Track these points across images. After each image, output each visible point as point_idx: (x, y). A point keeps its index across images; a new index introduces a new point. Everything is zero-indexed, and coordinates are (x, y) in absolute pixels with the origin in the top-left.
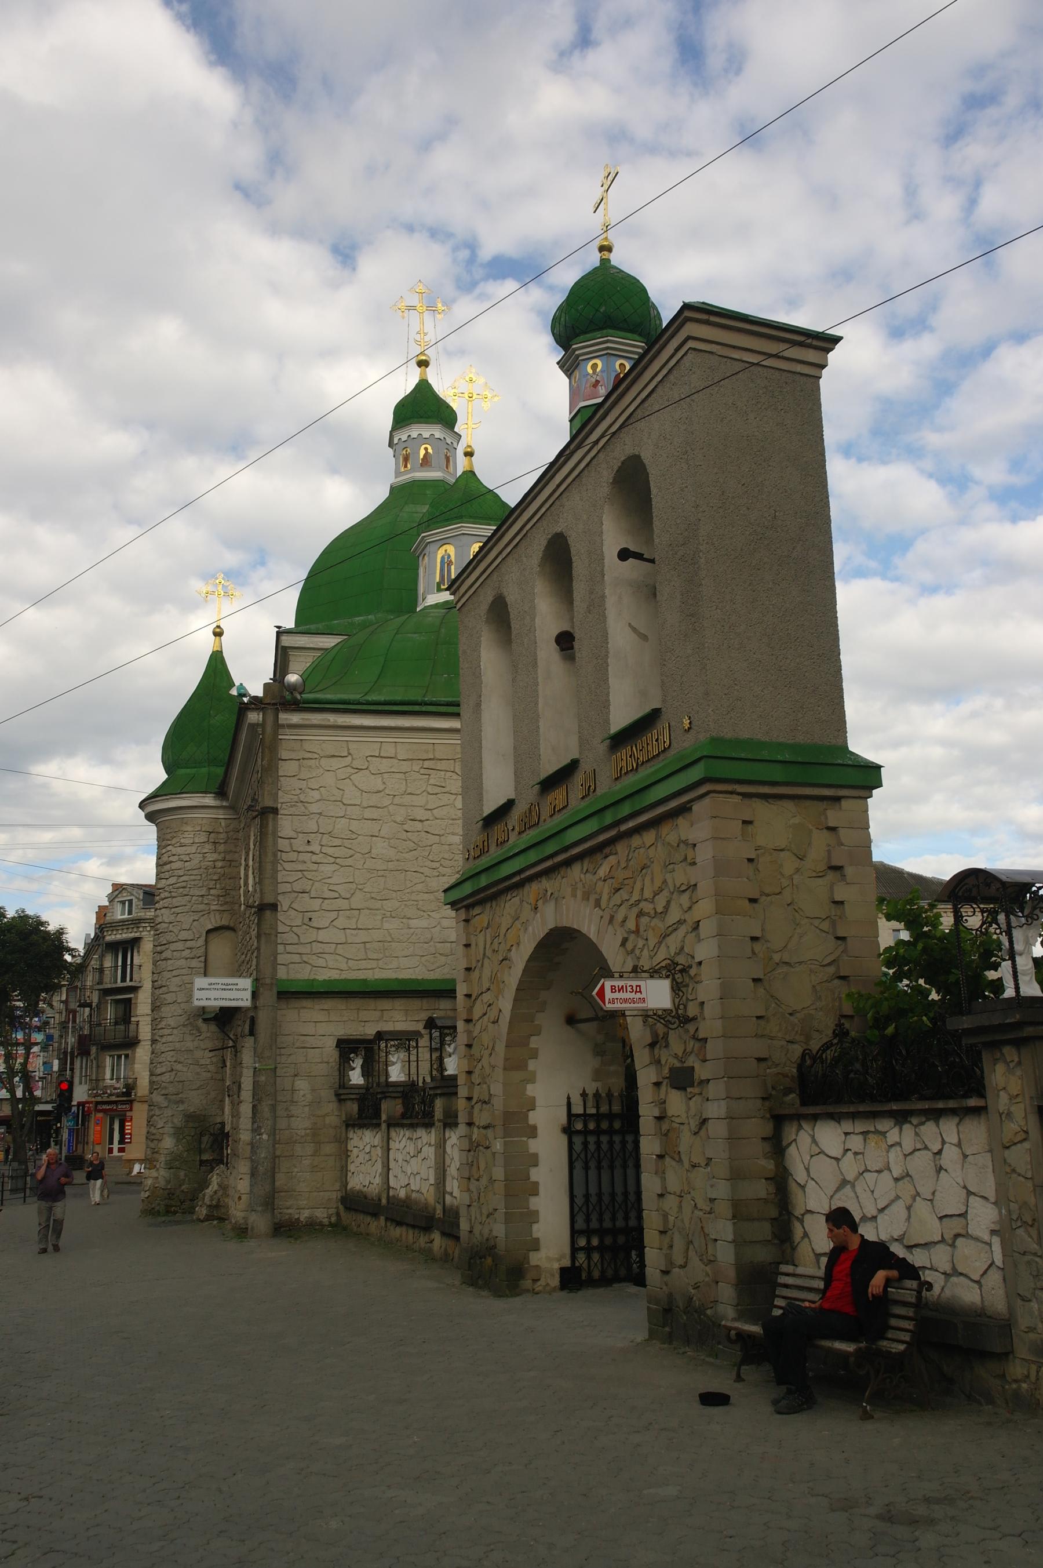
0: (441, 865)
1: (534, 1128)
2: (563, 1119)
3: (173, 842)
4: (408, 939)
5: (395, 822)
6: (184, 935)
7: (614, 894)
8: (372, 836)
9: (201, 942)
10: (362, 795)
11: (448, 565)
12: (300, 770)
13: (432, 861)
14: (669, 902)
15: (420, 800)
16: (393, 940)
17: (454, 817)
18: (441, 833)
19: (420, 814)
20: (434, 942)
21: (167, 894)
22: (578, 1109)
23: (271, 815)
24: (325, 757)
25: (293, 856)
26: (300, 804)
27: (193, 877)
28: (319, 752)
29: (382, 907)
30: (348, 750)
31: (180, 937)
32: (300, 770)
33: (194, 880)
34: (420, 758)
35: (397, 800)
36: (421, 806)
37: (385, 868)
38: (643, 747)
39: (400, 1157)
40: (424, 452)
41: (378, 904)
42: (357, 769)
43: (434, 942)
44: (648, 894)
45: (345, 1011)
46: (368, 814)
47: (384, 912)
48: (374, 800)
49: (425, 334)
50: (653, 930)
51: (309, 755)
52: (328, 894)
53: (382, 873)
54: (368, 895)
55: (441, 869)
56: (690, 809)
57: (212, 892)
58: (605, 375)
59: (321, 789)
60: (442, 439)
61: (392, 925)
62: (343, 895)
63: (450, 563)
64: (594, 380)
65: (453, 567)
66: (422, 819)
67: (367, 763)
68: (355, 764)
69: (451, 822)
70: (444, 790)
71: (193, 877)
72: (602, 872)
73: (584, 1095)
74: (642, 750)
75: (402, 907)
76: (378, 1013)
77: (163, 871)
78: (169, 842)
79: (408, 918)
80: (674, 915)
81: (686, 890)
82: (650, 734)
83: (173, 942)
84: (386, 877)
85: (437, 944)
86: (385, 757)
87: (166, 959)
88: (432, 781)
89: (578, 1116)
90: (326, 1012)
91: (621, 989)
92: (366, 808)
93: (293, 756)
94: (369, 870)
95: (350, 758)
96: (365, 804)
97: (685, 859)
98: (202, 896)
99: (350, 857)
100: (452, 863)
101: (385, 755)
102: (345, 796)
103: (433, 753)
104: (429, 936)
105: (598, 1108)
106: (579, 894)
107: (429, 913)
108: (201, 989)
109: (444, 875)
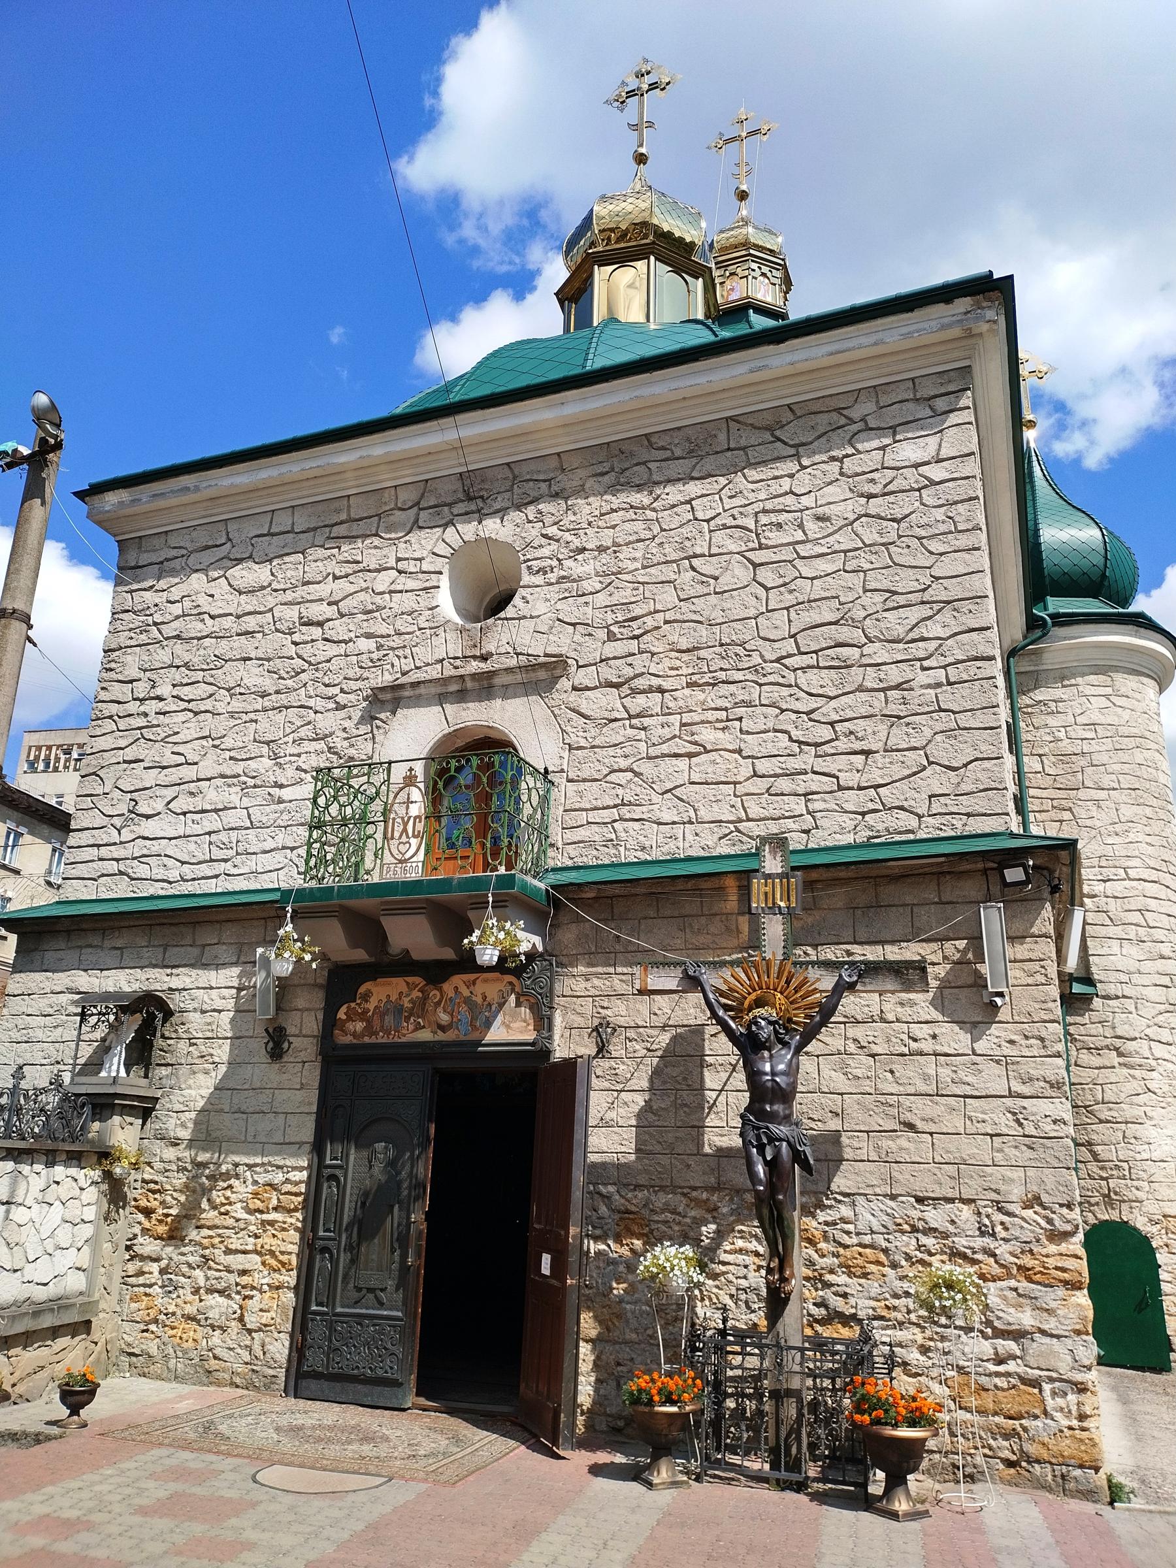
0: (342, 691)
13: (326, 686)
15: (323, 590)
17: (370, 607)
19: (318, 611)
24: (196, 551)
25: (133, 707)
28: (188, 545)
41: (238, 768)
42: (236, 559)
45: (145, 949)
51: (174, 553)
53: (252, 716)
54: (227, 754)
55: (342, 698)
62: (191, 758)
67: (250, 548)
69: (365, 617)
76: (195, 951)
79: (281, 786)
90: (119, 952)
93: (154, 558)
94: (232, 715)
95: (229, 545)
100: (359, 684)
103: (349, 511)
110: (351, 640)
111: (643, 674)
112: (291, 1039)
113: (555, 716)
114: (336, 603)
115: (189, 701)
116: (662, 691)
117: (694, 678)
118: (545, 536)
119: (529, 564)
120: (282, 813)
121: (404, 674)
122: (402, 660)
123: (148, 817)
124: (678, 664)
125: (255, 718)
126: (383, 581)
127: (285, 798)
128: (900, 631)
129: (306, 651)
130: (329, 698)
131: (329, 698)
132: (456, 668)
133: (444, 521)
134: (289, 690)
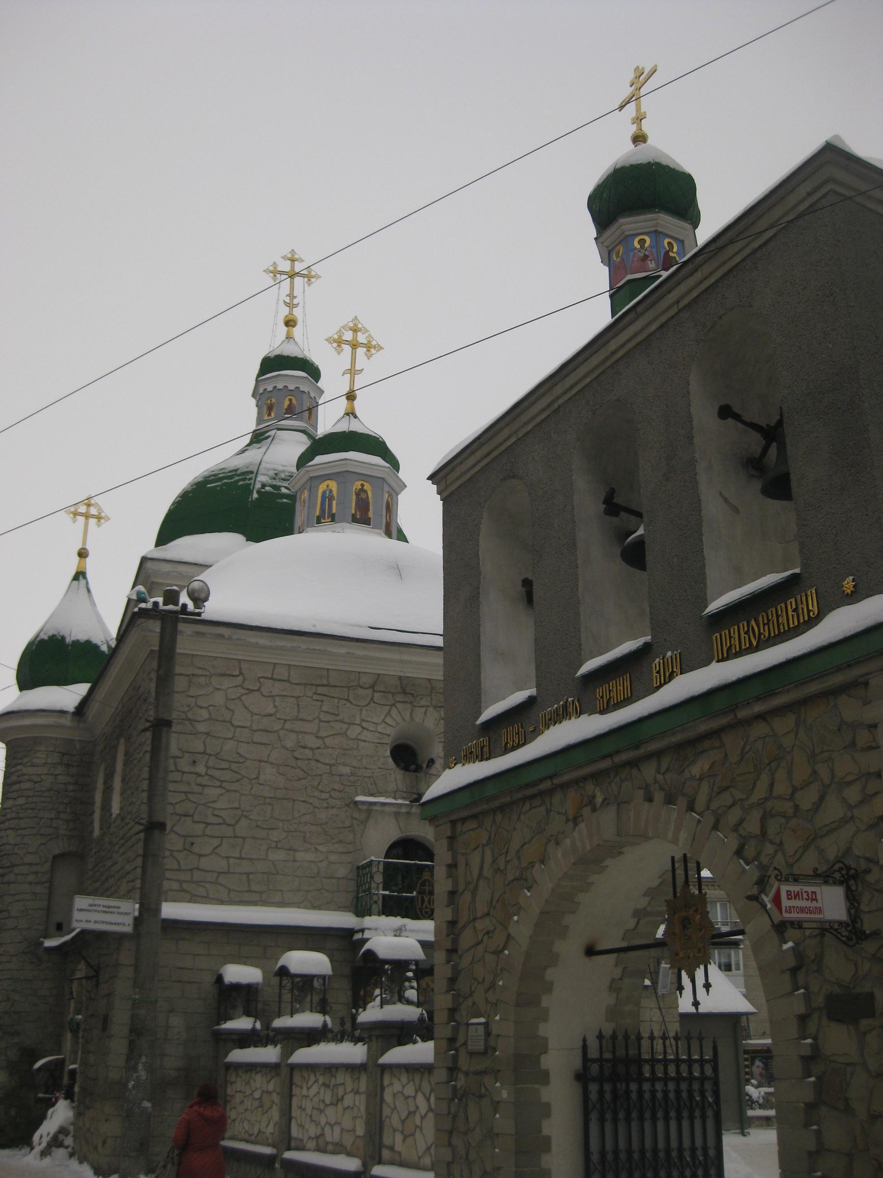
0: (330, 796)
1: (546, 1074)
2: (578, 1063)
3: (25, 760)
5: (285, 748)
6: (29, 859)
7: (718, 793)
8: (261, 761)
9: (47, 866)
11: (330, 499)
12: (189, 686)
13: (322, 792)
14: (822, 798)
17: (346, 747)
18: (333, 762)
19: (311, 741)
21: (14, 815)
22: (593, 1053)
23: (165, 729)
26: (187, 723)
27: (43, 799)
30: (240, 669)
31: (26, 860)
32: (189, 686)
33: (44, 802)
35: (288, 726)
38: (768, 620)
39: (308, 1106)
40: (288, 403)
42: (248, 689)
44: (781, 788)
46: (257, 737)
50: (794, 831)
51: (199, 672)
52: (211, 819)
55: (331, 801)
56: (866, 684)
57: (63, 816)
58: (654, 251)
59: (210, 708)
60: (307, 392)
61: (278, 856)
63: (331, 498)
64: (642, 255)
65: (334, 502)
67: (258, 684)
68: (247, 685)
71: (43, 799)
72: (696, 770)
73: (600, 1037)
74: (768, 624)
77: (11, 790)
78: (20, 761)
80: (833, 810)
81: (855, 780)
82: (783, 605)
83: (19, 865)
87: (9, 883)
88: (325, 708)
89: (594, 1061)
91: (797, 896)
92: (255, 731)
95: (241, 678)
96: (255, 727)
97: (853, 744)
98: (51, 819)
99: (237, 781)
105: (614, 1052)
106: (659, 796)
108: (81, 910)
109: (333, 807)
110: (334, 765)
112: (332, 1005)
115: (222, 781)
123: (200, 856)
130: (323, 800)
131: (323, 800)
133: (390, 703)
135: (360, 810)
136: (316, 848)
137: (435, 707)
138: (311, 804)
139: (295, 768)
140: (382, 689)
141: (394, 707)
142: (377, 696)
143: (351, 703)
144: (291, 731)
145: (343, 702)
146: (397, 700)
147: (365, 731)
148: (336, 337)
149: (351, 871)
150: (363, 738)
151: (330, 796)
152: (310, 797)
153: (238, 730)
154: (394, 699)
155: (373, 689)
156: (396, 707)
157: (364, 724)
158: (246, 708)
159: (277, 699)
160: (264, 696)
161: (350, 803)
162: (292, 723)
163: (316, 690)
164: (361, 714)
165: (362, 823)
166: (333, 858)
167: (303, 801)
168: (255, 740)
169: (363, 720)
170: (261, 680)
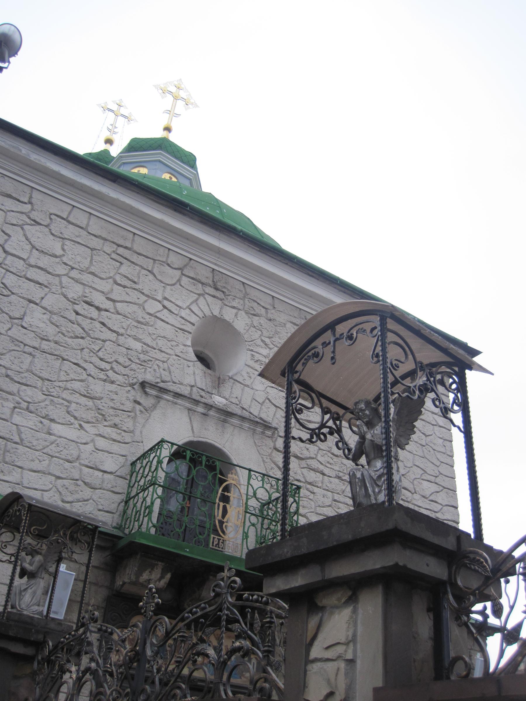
4: (44, 448)
5: (65, 296)
8: (30, 301)
10: (31, 251)
13: (101, 359)
15: (105, 286)
16: (21, 442)
17: (142, 320)
18: (121, 331)
19: (99, 299)
20: (80, 464)
29: (18, 393)
30: (31, 197)
34: (115, 241)
35: (74, 274)
36: (103, 292)
37: (37, 346)
41: (14, 387)
42: (34, 221)
43: (80, 464)
46: (32, 273)
47: (17, 399)
48: (44, 261)
49: (116, 127)
55: (110, 373)
66: (101, 306)
67: (49, 220)
68: (34, 215)
69: (136, 324)
70: (134, 286)
75: (47, 402)
79: (52, 420)
84: (34, 356)
85: (83, 468)
86: (73, 224)
94: (13, 340)
95: (29, 206)
96: (32, 261)
101: (74, 221)
102: (9, 243)
104: (75, 453)
107: (82, 423)
109: (112, 382)
110: (122, 335)
111: (313, 458)
113: (264, 461)
114: (114, 301)
116: (324, 474)
117: (341, 474)
118: (262, 341)
119: (253, 353)
120: (52, 443)
121: (163, 382)
122: (161, 370)
124: (331, 461)
125: (33, 353)
126: (153, 307)
127: (55, 432)
128: (427, 493)
129: (85, 323)
131: (102, 370)
132: (202, 397)
134: (67, 346)
135: (146, 393)
136: (80, 425)
137: (247, 313)
138: (85, 369)
139: (73, 323)
140: (192, 275)
141: (202, 298)
142: (185, 280)
143: (155, 276)
144: (77, 282)
145: (144, 272)
146: (207, 292)
147: (166, 310)
148: (162, 86)
149: (123, 466)
150: (163, 318)
151: (112, 368)
152: (86, 361)
153: (10, 257)
154: (204, 290)
155: (182, 272)
156: (205, 299)
157: (166, 303)
158: (27, 239)
159: (67, 242)
160: (53, 234)
161: (135, 384)
162: (80, 273)
163: (117, 249)
164: (164, 291)
165: (146, 410)
166: (101, 443)
167: (75, 364)
168: (28, 276)
169: (166, 298)
170: (53, 217)
